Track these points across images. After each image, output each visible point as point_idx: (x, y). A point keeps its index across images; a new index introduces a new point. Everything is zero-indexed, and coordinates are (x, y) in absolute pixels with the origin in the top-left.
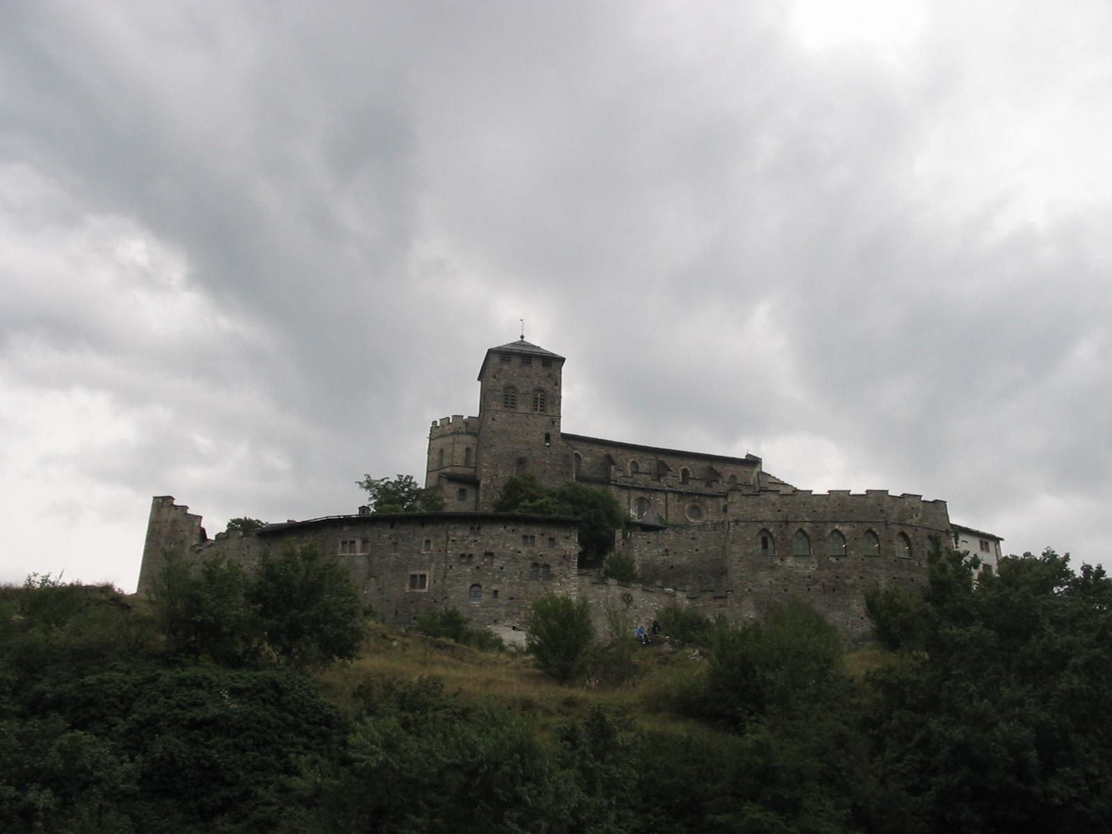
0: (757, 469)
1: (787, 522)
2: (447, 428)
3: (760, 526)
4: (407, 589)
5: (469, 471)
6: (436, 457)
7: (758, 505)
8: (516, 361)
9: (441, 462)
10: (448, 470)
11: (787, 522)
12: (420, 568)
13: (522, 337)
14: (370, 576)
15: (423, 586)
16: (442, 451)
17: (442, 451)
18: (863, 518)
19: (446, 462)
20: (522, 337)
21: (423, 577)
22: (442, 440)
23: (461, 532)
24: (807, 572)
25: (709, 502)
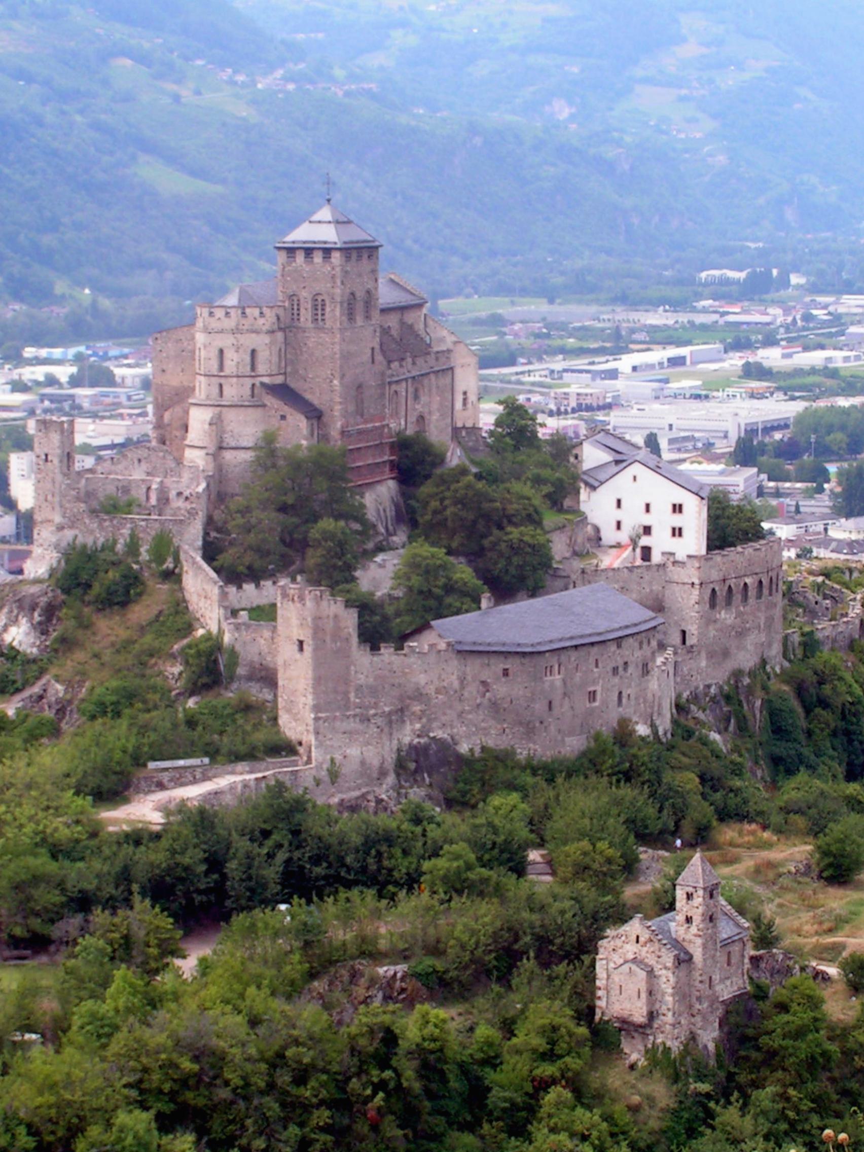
0: (425, 310)
1: (724, 580)
2: (261, 321)
3: (712, 586)
4: (588, 705)
5: (279, 380)
6: (248, 359)
7: (711, 567)
8: (354, 255)
9: (253, 368)
10: (266, 380)
11: (724, 580)
12: (594, 682)
14: (565, 694)
15: (594, 700)
16: (253, 352)
17: (253, 352)
18: (757, 571)
19: (262, 368)
21: (595, 692)
22: (254, 335)
23: (613, 647)
24: (729, 622)
25: (426, 382)
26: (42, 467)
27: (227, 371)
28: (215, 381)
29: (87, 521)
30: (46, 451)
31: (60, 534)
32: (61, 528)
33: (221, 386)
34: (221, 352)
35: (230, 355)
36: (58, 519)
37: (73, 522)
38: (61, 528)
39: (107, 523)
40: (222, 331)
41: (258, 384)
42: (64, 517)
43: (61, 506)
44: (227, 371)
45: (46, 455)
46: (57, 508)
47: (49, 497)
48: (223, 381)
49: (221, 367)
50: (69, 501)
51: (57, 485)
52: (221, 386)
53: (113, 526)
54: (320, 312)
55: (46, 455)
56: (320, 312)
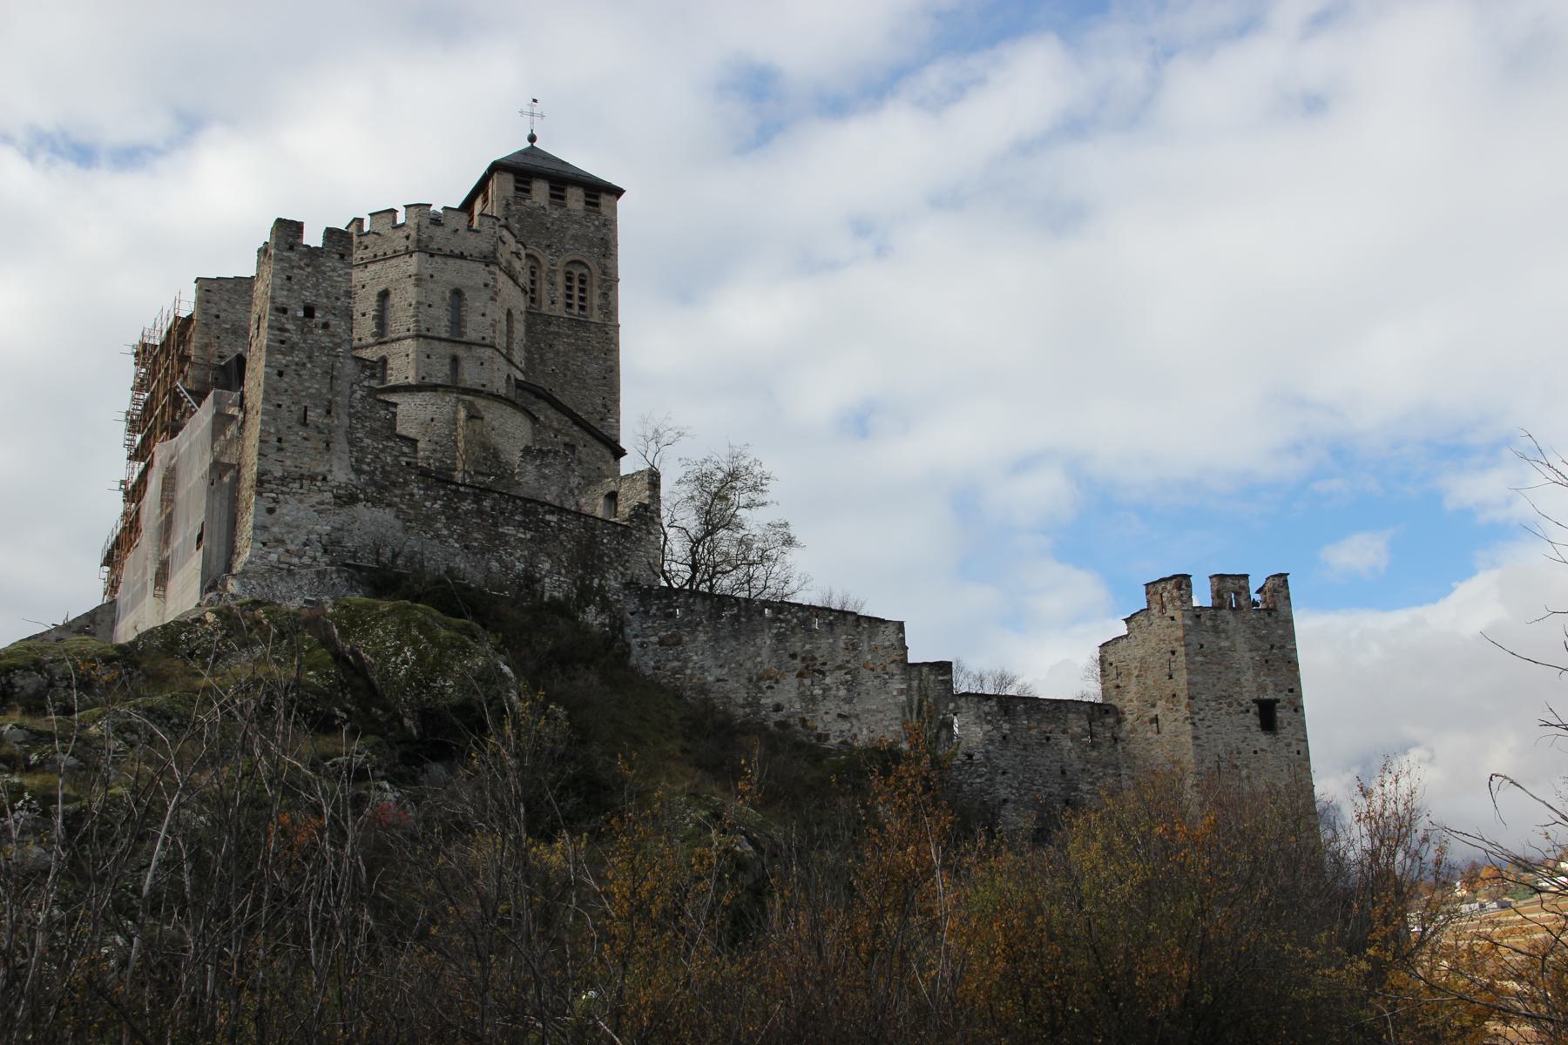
13: (532, 139)
20: (532, 139)
26: (295, 338)
27: (471, 334)
28: (446, 349)
29: (418, 493)
30: (309, 296)
31: (343, 516)
32: (347, 499)
33: (455, 360)
34: (457, 293)
35: (475, 302)
36: (341, 474)
37: (381, 488)
38: (347, 499)
39: (466, 506)
40: (462, 256)
41: (513, 378)
42: (358, 472)
43: (351, 443)
44: (471, 334)
45: (309, 311)
46: (341, 444)
47: (312, 415)
48: (461, 352)
49: (457, 323)
50: (373, 433)
51: (342, 385)
52: (455, 360)
53: (480, 512)
54: (576, 293)
55: (309, 311)
56: (576, 293)
